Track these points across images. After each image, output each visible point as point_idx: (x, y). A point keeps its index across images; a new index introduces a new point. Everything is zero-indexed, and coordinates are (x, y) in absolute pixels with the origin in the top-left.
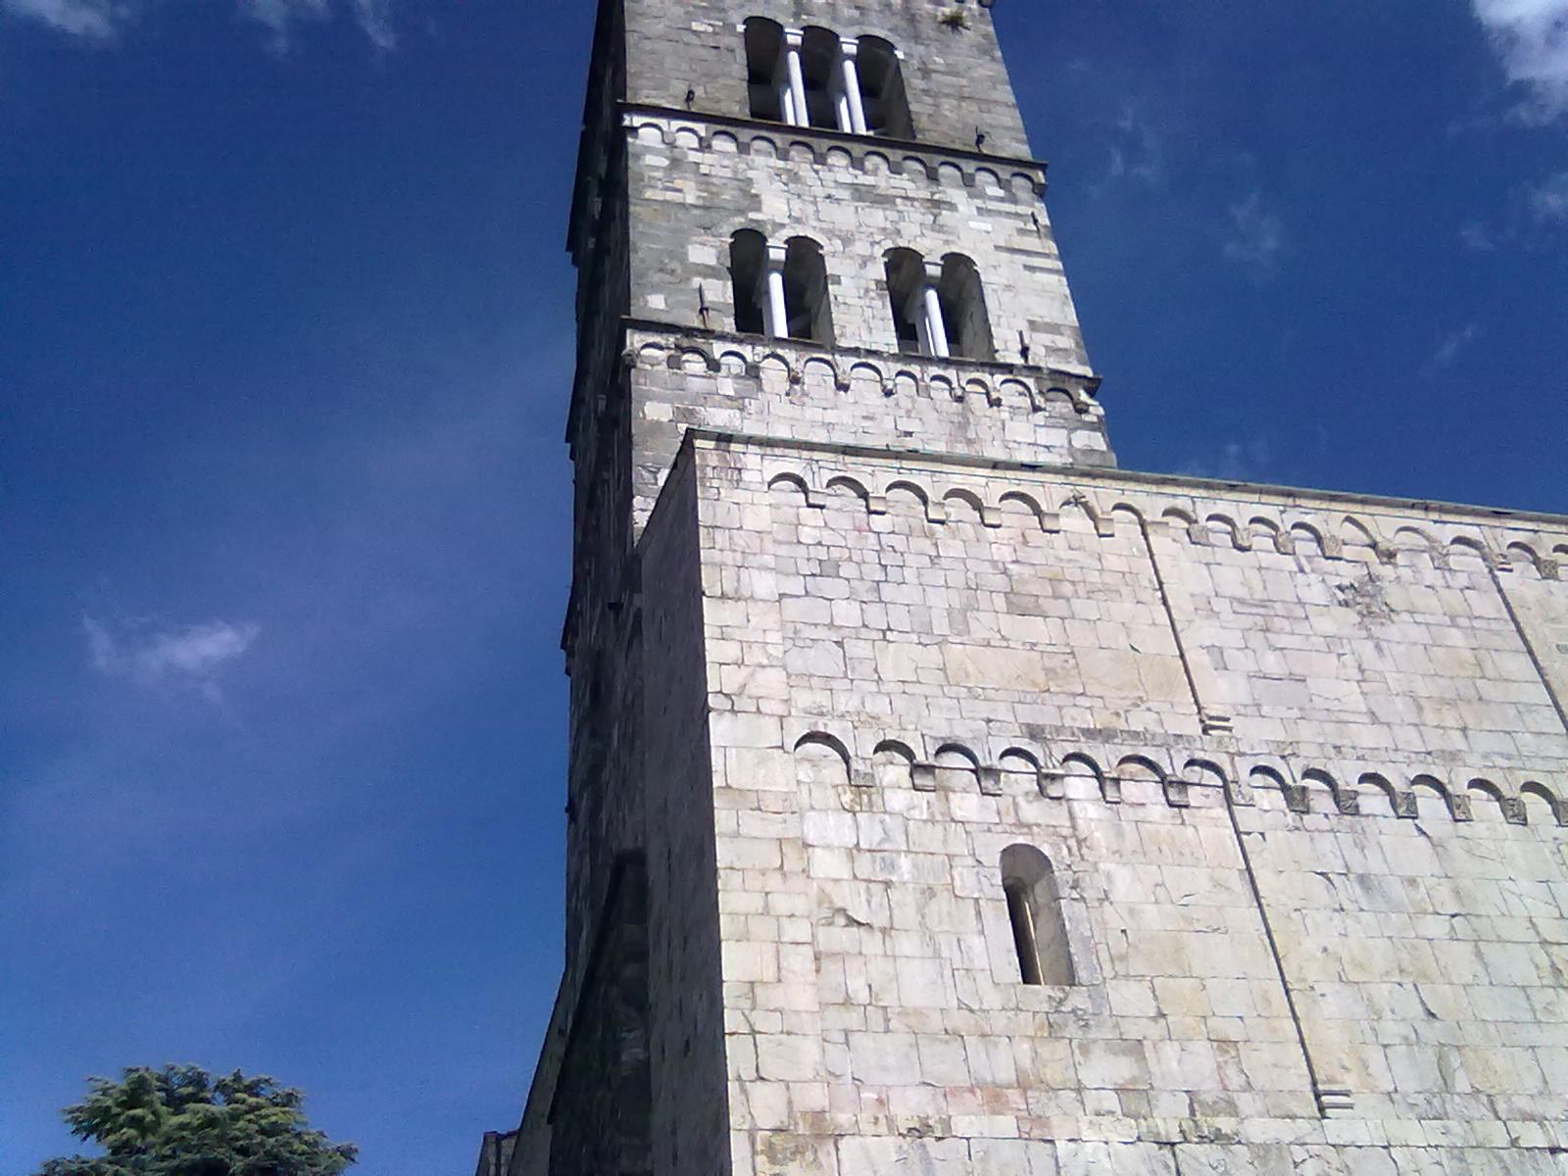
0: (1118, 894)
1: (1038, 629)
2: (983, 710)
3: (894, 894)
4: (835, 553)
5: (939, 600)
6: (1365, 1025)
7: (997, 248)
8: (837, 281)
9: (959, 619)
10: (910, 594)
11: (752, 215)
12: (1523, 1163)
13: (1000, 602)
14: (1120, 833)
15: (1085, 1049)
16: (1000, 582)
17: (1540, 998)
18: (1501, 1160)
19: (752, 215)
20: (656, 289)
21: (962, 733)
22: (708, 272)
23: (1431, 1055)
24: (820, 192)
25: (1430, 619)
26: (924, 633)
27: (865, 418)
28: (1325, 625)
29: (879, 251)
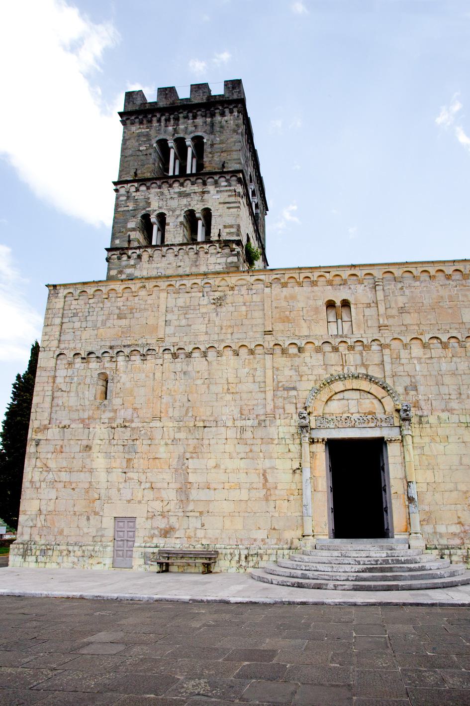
1: (123, 322)
2: (103, 343)
4: (78, 310)
5: (100, 319)
9: (104, 323)
10: (94, 318)
13: (116, 317)
16: (117, 311)
17: (219, 396)
18: (190, 429)
21: (94, 350)
23: (185, 409)
26: (95, 328)
27: (168, 264)
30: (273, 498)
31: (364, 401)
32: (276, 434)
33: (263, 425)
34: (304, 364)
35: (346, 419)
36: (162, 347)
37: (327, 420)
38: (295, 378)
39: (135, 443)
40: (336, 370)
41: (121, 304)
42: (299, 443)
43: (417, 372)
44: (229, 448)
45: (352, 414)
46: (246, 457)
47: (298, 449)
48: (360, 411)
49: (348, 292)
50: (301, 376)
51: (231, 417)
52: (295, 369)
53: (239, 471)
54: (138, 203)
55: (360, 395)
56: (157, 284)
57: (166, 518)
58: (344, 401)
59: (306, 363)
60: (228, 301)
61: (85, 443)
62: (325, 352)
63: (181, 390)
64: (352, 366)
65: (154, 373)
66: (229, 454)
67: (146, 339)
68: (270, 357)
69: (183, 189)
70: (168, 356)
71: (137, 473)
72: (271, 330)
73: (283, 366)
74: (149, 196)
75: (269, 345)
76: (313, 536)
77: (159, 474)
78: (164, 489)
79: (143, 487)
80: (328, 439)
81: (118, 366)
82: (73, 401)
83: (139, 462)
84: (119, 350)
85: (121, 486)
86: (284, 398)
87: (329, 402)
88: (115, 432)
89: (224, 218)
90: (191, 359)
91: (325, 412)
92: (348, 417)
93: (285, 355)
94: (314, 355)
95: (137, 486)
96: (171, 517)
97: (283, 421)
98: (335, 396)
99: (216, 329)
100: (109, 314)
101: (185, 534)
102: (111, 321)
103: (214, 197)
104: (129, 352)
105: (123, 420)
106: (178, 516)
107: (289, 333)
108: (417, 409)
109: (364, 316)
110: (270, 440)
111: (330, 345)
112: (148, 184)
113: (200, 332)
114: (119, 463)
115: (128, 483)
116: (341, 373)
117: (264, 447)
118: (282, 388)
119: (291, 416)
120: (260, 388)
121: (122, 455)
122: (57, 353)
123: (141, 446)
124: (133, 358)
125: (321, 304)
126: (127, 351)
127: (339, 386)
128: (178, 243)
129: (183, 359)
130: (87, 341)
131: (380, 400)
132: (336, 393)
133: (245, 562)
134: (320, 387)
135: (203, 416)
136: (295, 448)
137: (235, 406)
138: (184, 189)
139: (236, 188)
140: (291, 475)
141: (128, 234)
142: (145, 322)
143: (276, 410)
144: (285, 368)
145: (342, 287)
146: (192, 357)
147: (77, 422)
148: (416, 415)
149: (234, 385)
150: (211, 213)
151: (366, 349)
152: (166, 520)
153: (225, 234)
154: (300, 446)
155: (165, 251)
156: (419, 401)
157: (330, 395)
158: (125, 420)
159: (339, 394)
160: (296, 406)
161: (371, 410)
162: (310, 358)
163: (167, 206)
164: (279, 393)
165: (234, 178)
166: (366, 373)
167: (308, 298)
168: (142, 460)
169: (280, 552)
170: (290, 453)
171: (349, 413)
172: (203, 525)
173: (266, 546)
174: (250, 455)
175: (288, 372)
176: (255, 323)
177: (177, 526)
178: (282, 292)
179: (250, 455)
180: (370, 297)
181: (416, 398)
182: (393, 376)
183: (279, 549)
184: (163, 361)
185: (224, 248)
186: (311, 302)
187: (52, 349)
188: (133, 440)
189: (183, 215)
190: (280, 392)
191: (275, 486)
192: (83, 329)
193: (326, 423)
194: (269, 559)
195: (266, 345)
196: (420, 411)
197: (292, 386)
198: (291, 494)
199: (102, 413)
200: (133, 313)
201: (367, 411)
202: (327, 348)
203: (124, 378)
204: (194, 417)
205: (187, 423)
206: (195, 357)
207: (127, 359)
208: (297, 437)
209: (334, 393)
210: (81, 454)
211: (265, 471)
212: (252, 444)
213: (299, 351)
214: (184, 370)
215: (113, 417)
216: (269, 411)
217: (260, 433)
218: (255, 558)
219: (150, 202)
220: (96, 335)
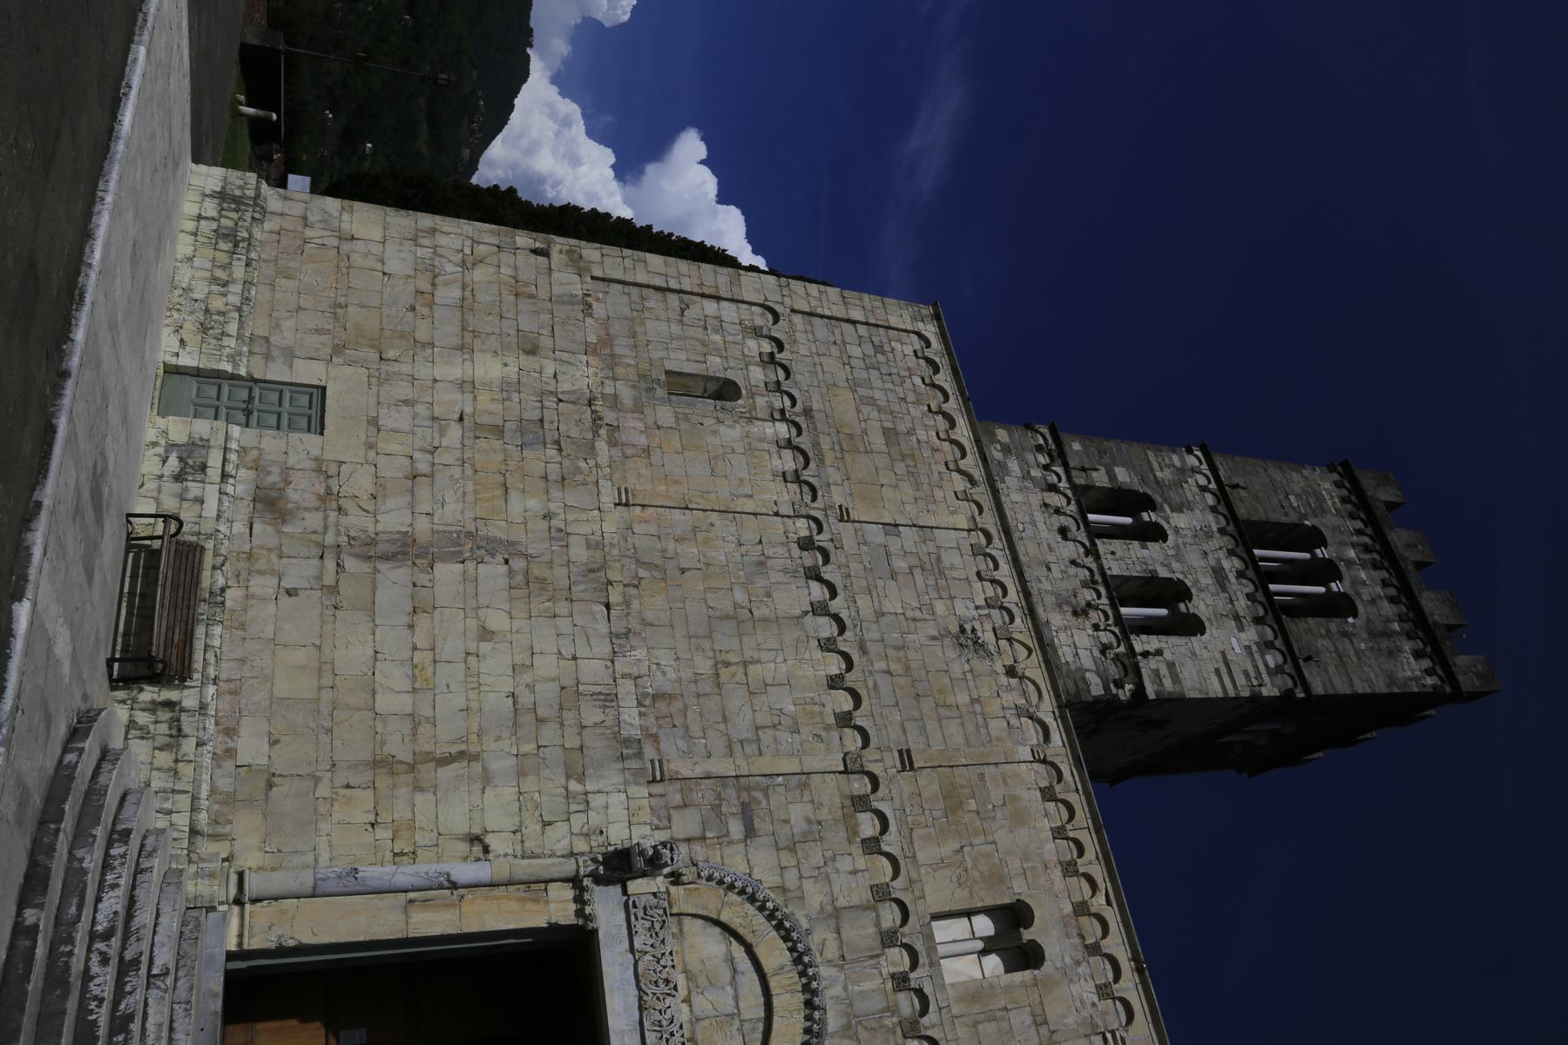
0: (722, 428)
1: (878, 441)
2: (816, 397)
3: (700, 330)
4: (890, 355)
5: (877, 394)
6: (670, 531)
7: (1223, 653)
8: (1145, 547)
9: (871, 401)
10: (877, 383)
11: (1166, 507)
12: (598, 582)
13: (888, 425)
14: (762, 440)
15: (634, 387)
17: (706, 644)
19: (1166, 507)
20: (1084, 446)
22: (1112, 476)
23: (659, 562)
24: (1206, 548)
25: (971, 684)
28: (940, 607)
29: (1181, 577)
30: (383, 782)
32: (601, 785)
33: (625, 751)
34: (829, 854)
35: (667, 981)
36: (826, 516)
37: (657, 926)
38: (784, 832)
39: (548, 446)
40: (822, 941)
41: (923, 437)
44: (546, 665)
46: (519, 706)
47: (555, 847)
48: (699, 1027)
49: (1068, 960)
50: (792, 849)
51: (644, 670)
52: (810, 832)
53: (473, 689)
54: (1174, 488)
56: (986, 509)
57: (318, 504)
58: (729, 975)
59: (834, 859)
60: (976, 663)
61: (546, 342)
62: (875, 909)
63: (712, 554)
64: (845, 989)
65: (751, 496)
66: (528, 662)
67: (840, 482)
68: (837, 765)
69: (1232, 577)
70: (802, 528)
71: (460, 446)
72: (916, 765)
73: (816, 800)
74: (1197, 511)
75: (871, 762)
76: (238, 901)
77: (460, 493)
78: (412, 506)
79: (417, 455)
80: (595, 932)
81: (761, 423)
82: (655, 328)
83: (495, 452)
84: (804, 426)
85: (420, 408)
86: (720, 805)
87: (717, 930)
88: (578, 407)
89: (1189, 661)
90: (803, 580)
92: (675, 988)
93: (848, 803)
94: (865, 881)
95: (419, 444)
96: (320, 515)
97: (645, 802)
98: (742, 949)
99: (894, 635)
100: (892, 412)
101: (262, 547)
102: (875, 415)
103: (1233, 639)
104: (803, 446)
105: (615, 424)
106: (325, 534)
107: (917, 810)
109: (1006, 1009)
110: (580, 770)
111: (898, 923)
112: (1221, 509)
113: (879, 602)
114: (488, 407)
115: (429, 423)
117: (553, 754)
118: (747, 800)
119: (661, 825)
120: (741, 742)
121: (514, 413)
122: (778, 308)
123: (542, 460)
124: (788, 454)
125: (1019, 889)
126: (804, 441)
127: (775, 954)
128: (1106, 565)
129: (799, 561)
130: (819, 368)
133: (153, 702)
134: (765, 901)
135: (641, 604)
136: (559, 839)
137: (679, 680)
138: (1233, 580)
139: (1269, 686)
140: (462, 827)
141: (1098, 467)
142: (884, 481)
143: (678, 785)
144: (809, 806)
145: (1077, 941)
146: (810, 582)
147: (602, 333)
149: (740, 677)
150: (1195, 635)
151: (905, 1024)
152: (311, 501)
153: (1154, 666)
154: (565, 852)
155: (1079, 538)
157: (741, 931)
158: (613, 428)
162: (850, 868)
163: (1184, 544)
164: (731, 793)
165: (1290, 683)
167: (1026, 857)
168: (500, 457)
169: (184, 802)
170: (538, 828)
172: (290, 593)
173: (207, 761)
174: (528, 718)
175: (798, 813)
176: (928, 727)
177: (288, 529)
178: (1029, 789)
179: (521, 715)
180: (1066, 1021)
183: (194, 798)
184: (789, 517)
185: (1119, 664)
186: (1015, 864)
187: (786, 299)
188: (557, 443)
189: (1173, 576)
190: (735, 795)
191: (425, 785)
192: (846, 360)
193: (648, 924)
194: (158, 769)
195: (870, 754)
197: (757, 826)
198: (395, 832)
199: (630, 383)
200: (903, 460)
202: (890, 916)
203: (731, 433)
204: (636, 582)
205: (618, 565)
206: (809, 588)
207: (782, 443)
208: (594, 844)
209: (749, 938)
210: (513, 332)
211: (475, 757)
212: (562, 724)
213: (863, 841)
214: (770, 563)
215: (621, 404)
216: (672, 766)
217: (597, 745)
218: (163, 728)
219: (1183, 512)
220: (835, 385)
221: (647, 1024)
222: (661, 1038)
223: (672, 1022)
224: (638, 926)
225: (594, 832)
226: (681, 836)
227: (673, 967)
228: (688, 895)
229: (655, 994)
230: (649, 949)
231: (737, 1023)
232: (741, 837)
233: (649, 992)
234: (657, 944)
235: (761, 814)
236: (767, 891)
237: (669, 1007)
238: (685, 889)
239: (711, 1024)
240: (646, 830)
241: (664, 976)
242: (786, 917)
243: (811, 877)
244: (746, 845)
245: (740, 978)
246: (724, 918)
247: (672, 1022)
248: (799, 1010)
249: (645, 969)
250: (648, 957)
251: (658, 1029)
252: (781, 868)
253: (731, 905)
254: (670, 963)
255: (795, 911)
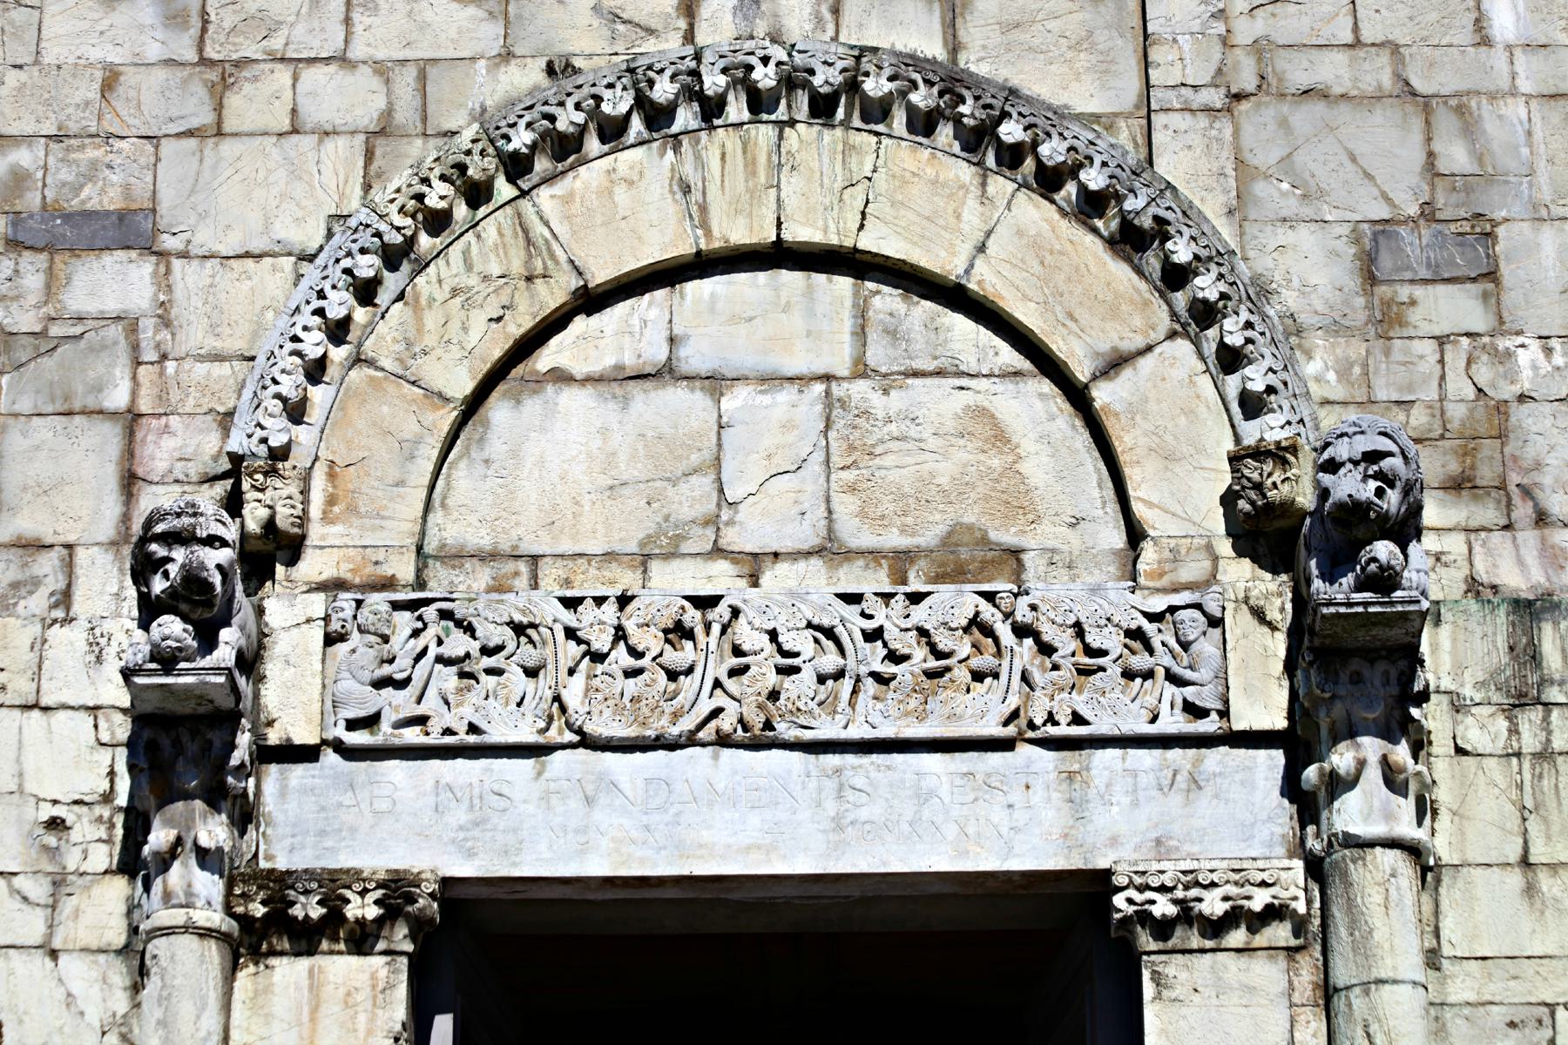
31: (897, 400)
35: (679, 632)
37: (459, 643)
42: (118, 938)
43: (1498, 58)
45: (754, 566)
47: (94, 1016)
55: (861, 333)
58: (676, 397)
87: (498, 410)
91: (447, 530)
92: (705, 603)
98: (580, 324)
108: (1488, 513)
116: (671, 45)
119: (55, 582)
131: (1078, 396)
132: (591, 300)
148: (1474, 586)
154: (119, 974)
156: (1521, 415)
157: (520, 323)
159: (620, 311)
160: (129, 453)
161: (969, 519)
166: (934, 48)
171: (718, 551)
181: (1484, 373)
182: (1238, 97)
193: (448, 679)
196: (1528, 538)
201: (929, 537)
209: (553, 295)
221: (827, 730)
222: (881, 679)
223: (830, 633)
224: (449, 720)
225: (52, 852)
226: (112, 507)
227: (624, 601)
228: (352, 510)
229: (717, 684)
230: (544, 687)
231: (860, 389)
232: (146, 268)
233: (705, 707)
234: (528, 654)
235: (66, 175)
236: (379, 196)
237: (773, 635)
238: (326, 518)
239: (852, 489)
240: (68, 642)
241: (650, 641)
242: (492, 135)
243: (347, 21)
244: (184, 255)
245: (694, 358)
246: (463, 386)
247: (830, 633)
248: (848, 149)
249: (619, 710)
250: (573, 693)
251: (847, 685)
252: (295, 131)
253: (411, 348)
254: (610, 609)
255: (473, 103)
